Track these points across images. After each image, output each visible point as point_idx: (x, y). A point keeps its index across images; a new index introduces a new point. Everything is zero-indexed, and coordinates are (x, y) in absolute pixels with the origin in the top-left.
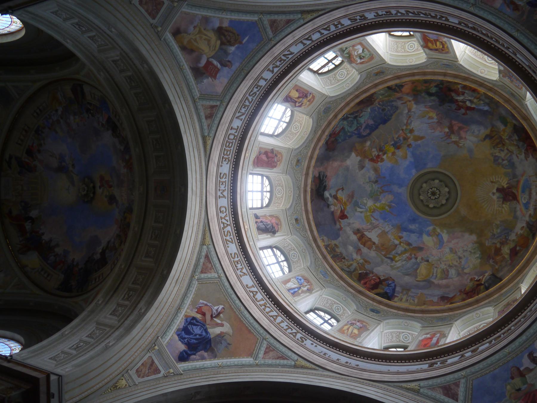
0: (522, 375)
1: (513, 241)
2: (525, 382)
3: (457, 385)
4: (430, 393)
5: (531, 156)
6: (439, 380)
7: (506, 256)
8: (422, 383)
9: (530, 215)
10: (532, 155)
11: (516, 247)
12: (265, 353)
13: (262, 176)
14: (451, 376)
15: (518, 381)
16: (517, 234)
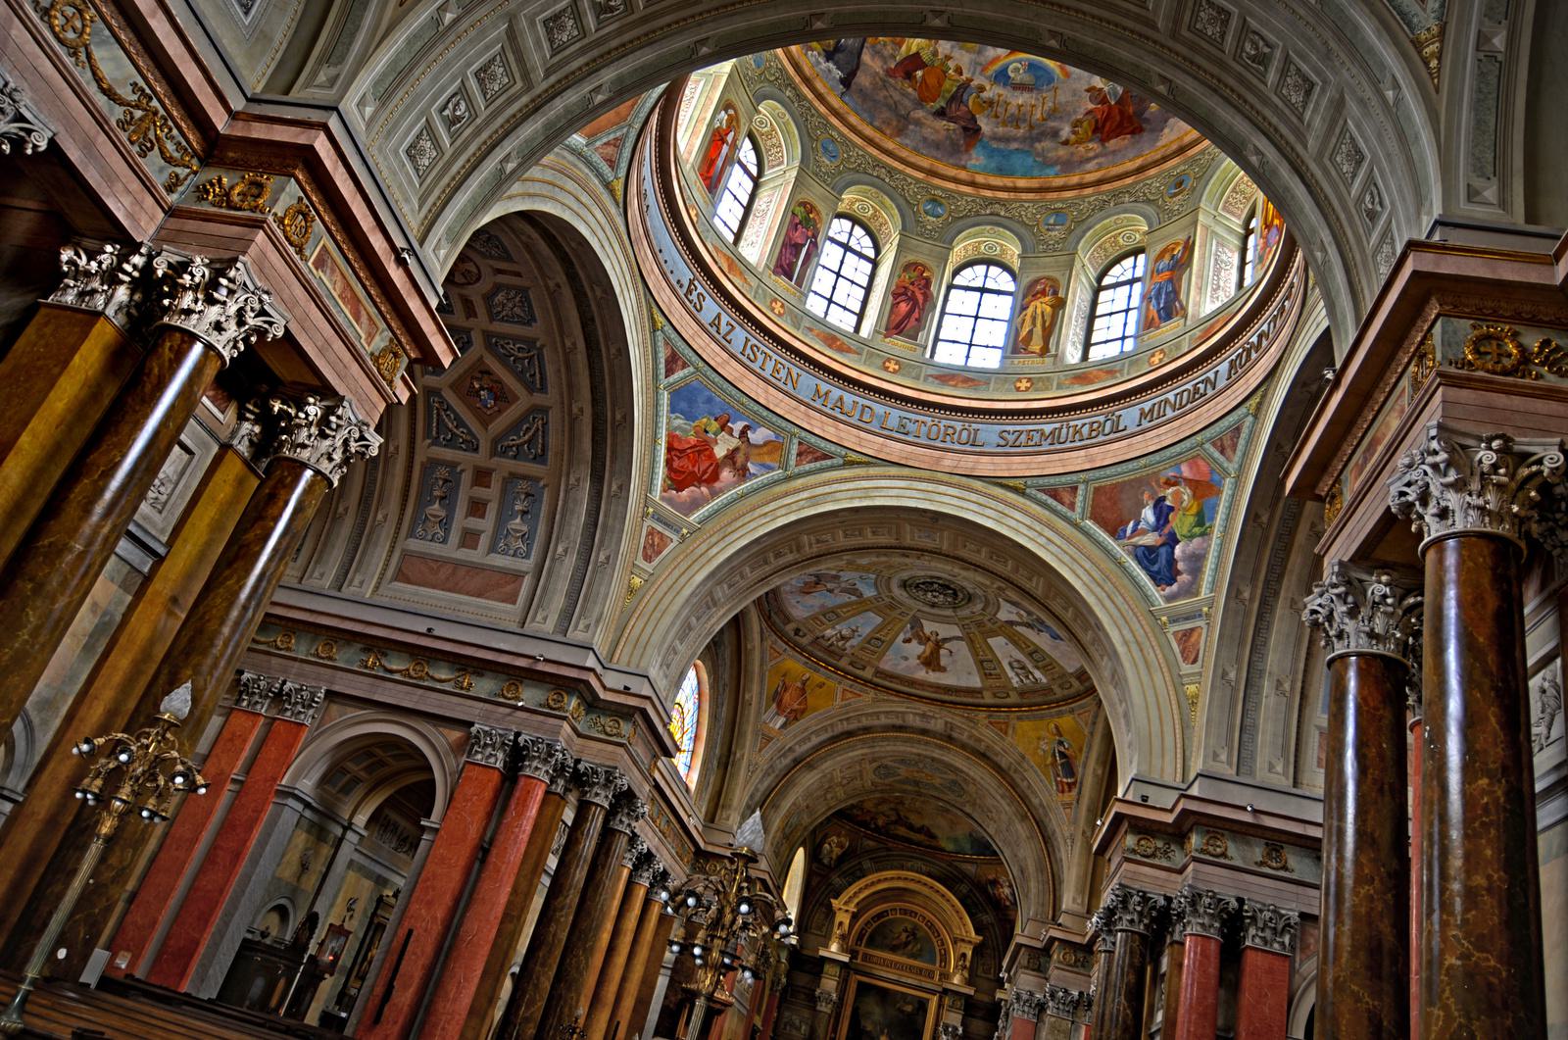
0: (723, 428)
1: (935, 53)
2: (716, 434)
3: (684, 366)
4: (661, 344)
5: (1091, 106)
6: (680, 343)
7: (904, 48)
8: (668, 328)
9: (982, 89)
10: (1089, 112)
11: (922, 65)
12: (607, 144)
13: (950, 287)
14: (691, 354)
15: (715, 425)
16: (948, 58)
